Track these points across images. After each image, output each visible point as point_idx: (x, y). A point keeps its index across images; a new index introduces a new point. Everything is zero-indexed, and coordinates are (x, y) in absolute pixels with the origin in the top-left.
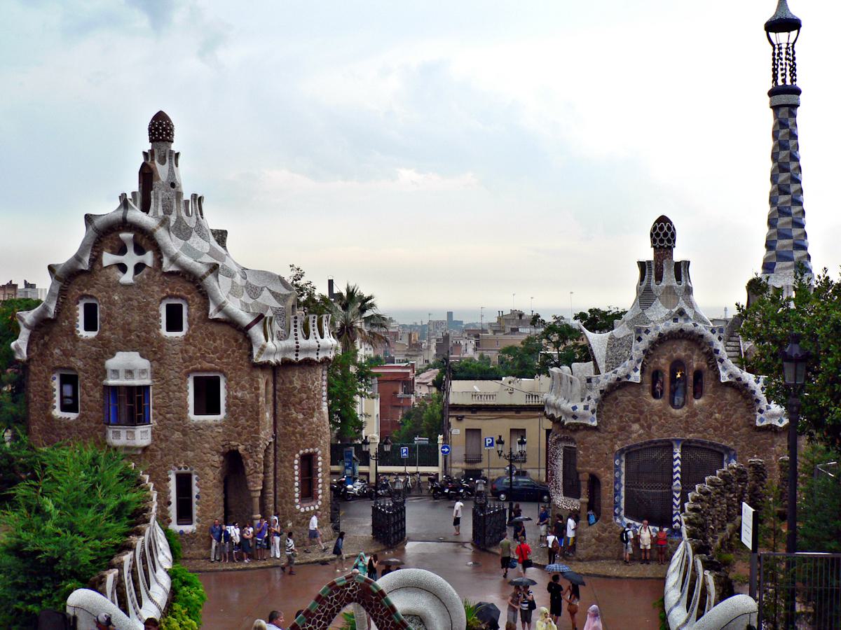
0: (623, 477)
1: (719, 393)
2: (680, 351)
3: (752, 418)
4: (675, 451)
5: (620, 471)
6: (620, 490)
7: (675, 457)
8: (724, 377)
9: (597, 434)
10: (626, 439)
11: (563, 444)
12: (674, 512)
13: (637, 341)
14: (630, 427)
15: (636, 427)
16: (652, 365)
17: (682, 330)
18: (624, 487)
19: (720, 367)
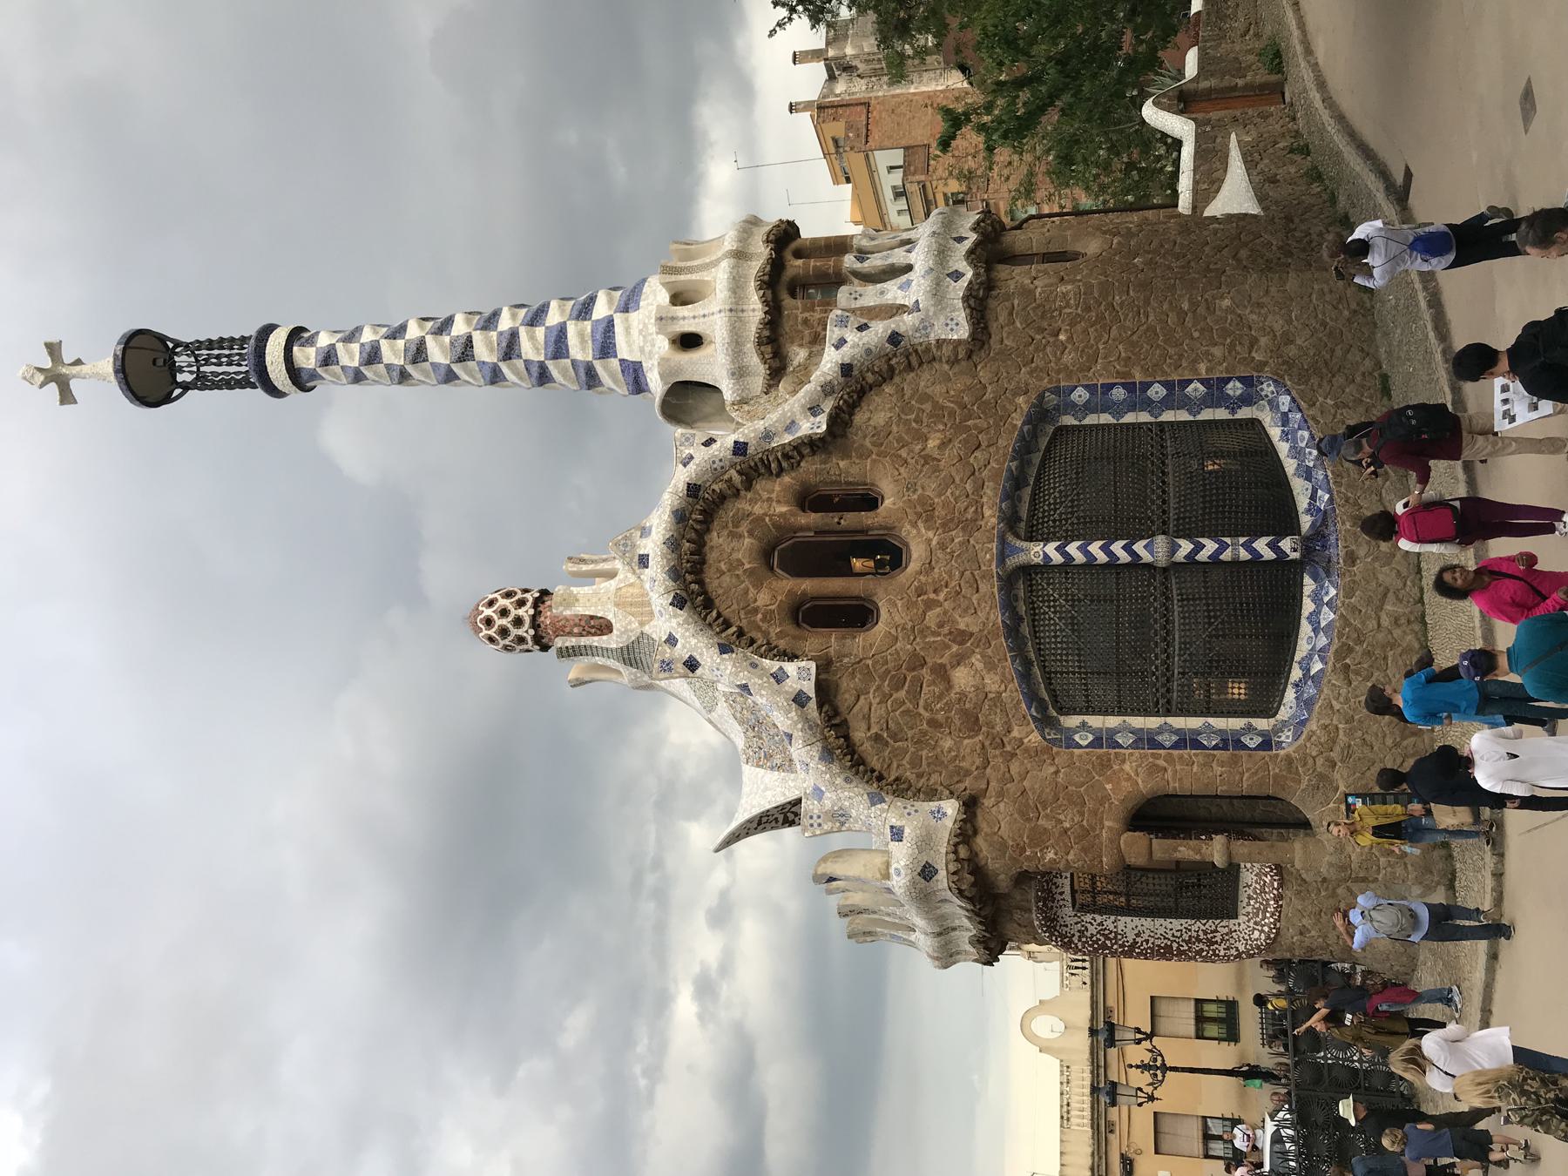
0: (1137, 722)
1: (867, 443)
2: (732, 549)
3: (947, 351)
4: (1039, 560)
5: (1112, 732)
6: (1177, 732)
7: (1057, 559)
8: (815, 426)
9: (988, 802)
10: (1005, 711)
11: (1067, 913)
12: (1244, 555)
13: (699, 672)
14: (963, 696)
15: (962, 678)
16: (774, 631)
17: (673, 544)
18: (1170, 720)
19: (787, 438)
